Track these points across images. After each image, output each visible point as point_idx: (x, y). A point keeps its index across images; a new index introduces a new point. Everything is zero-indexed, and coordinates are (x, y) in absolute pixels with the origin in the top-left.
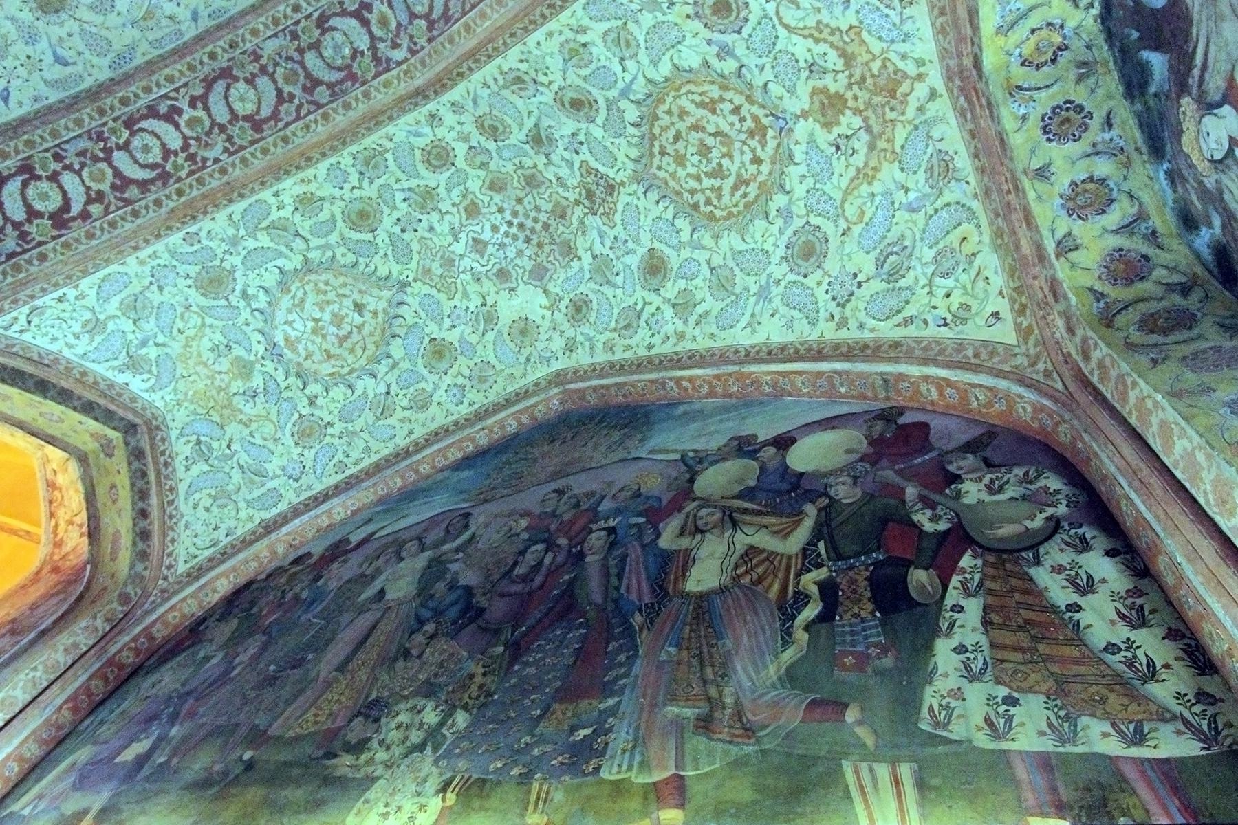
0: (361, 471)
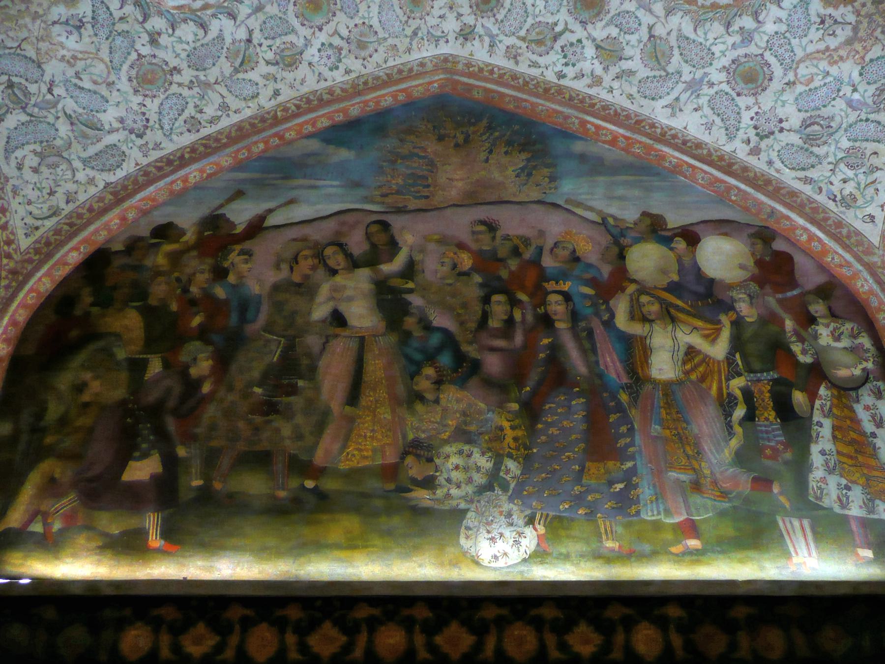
0: (220, 132)
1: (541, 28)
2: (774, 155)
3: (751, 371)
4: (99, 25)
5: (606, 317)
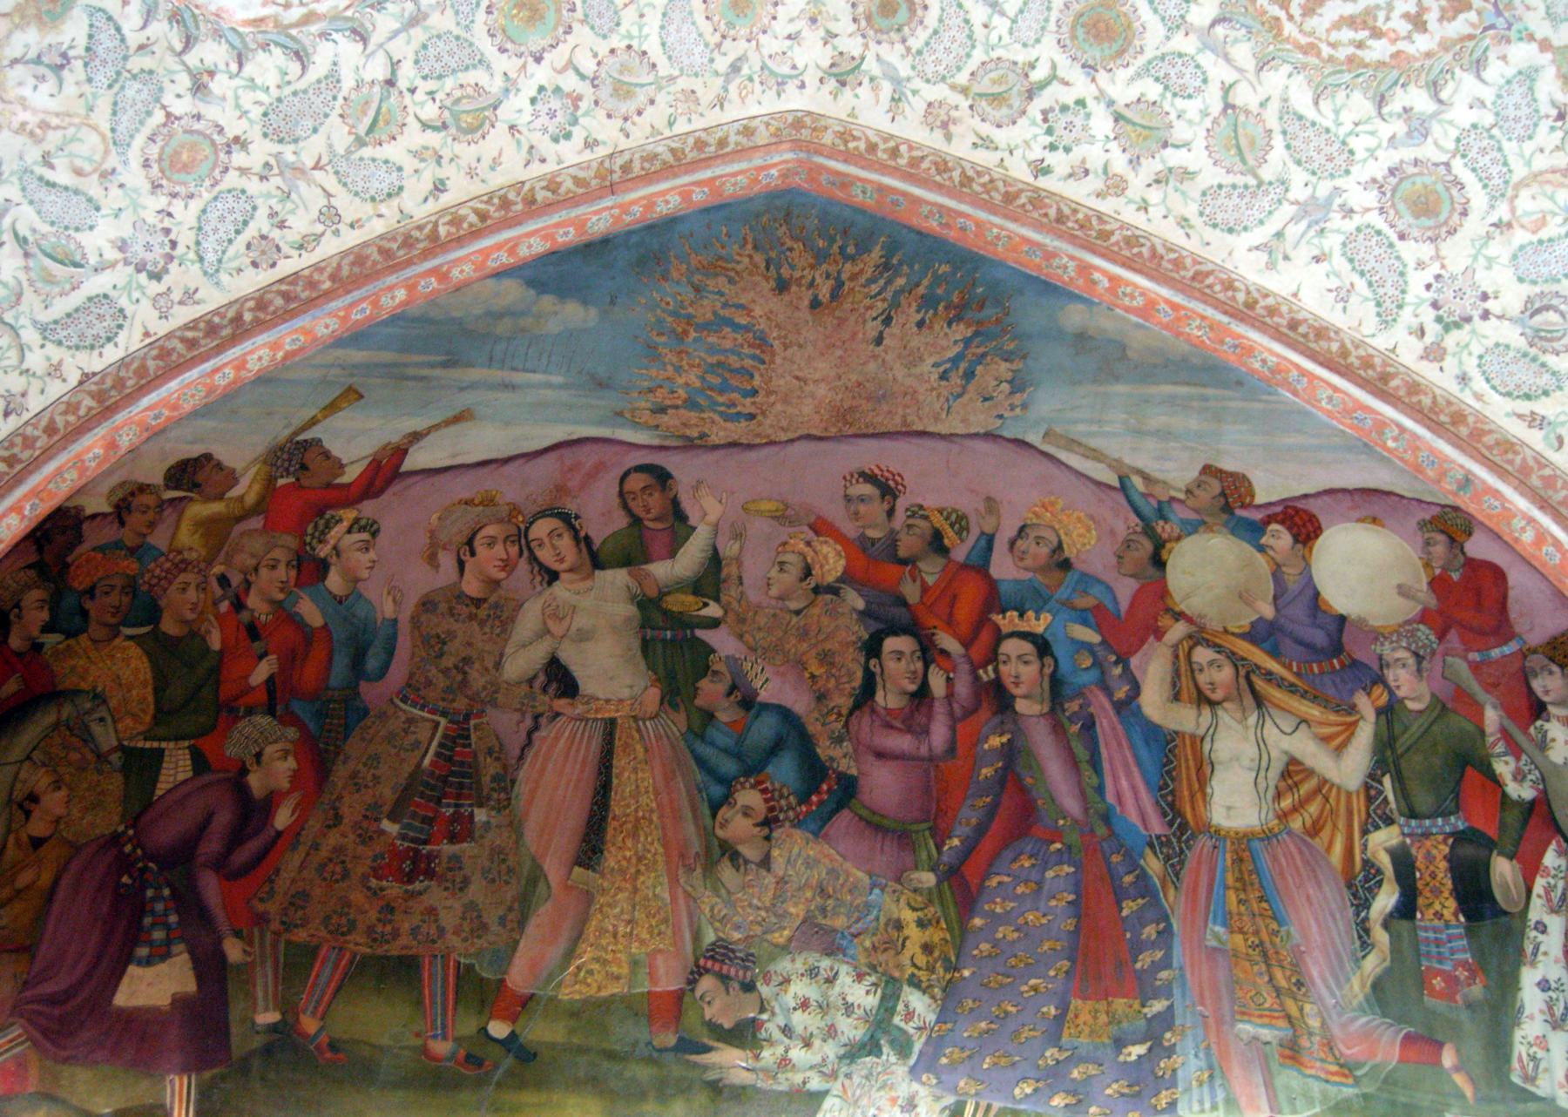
0: (317, 268)
1: (1001, 72)
2: (1471, 366)
3: (1412, 814)
4: (97, 62)
5: (1120, 694)
